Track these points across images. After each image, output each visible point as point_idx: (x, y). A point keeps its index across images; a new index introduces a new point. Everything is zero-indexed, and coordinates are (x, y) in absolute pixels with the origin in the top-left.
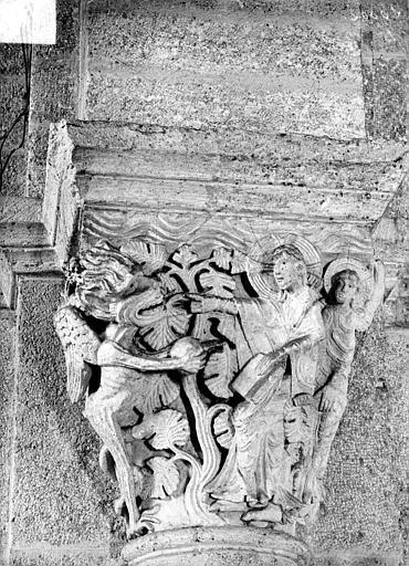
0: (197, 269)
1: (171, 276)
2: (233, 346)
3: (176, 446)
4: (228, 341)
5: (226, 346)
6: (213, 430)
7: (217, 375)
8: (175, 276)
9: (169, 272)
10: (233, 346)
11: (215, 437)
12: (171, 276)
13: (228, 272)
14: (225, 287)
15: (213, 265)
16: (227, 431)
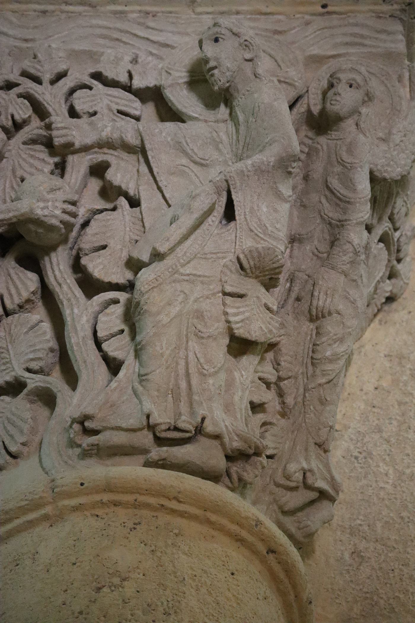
0: (66, 84)
1: (20, 96)
2: (134, 203)
3: (29, 370)
4: (126, 195)
5: (123, 202)
6: (95, 332)
7: (104, 247)
8: (28, 97)
9: (16, 90)
10: (134, 203)
11: (98, 344)
12: (20, 96)
13: (128, 88)
14: (119, 112)
15: (97, 76)
16: (122, 331)
